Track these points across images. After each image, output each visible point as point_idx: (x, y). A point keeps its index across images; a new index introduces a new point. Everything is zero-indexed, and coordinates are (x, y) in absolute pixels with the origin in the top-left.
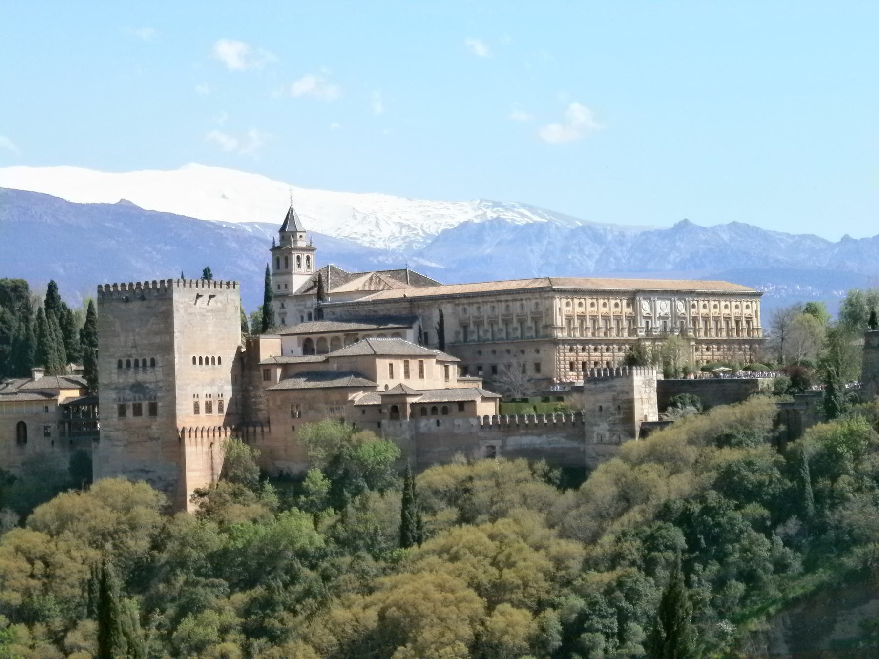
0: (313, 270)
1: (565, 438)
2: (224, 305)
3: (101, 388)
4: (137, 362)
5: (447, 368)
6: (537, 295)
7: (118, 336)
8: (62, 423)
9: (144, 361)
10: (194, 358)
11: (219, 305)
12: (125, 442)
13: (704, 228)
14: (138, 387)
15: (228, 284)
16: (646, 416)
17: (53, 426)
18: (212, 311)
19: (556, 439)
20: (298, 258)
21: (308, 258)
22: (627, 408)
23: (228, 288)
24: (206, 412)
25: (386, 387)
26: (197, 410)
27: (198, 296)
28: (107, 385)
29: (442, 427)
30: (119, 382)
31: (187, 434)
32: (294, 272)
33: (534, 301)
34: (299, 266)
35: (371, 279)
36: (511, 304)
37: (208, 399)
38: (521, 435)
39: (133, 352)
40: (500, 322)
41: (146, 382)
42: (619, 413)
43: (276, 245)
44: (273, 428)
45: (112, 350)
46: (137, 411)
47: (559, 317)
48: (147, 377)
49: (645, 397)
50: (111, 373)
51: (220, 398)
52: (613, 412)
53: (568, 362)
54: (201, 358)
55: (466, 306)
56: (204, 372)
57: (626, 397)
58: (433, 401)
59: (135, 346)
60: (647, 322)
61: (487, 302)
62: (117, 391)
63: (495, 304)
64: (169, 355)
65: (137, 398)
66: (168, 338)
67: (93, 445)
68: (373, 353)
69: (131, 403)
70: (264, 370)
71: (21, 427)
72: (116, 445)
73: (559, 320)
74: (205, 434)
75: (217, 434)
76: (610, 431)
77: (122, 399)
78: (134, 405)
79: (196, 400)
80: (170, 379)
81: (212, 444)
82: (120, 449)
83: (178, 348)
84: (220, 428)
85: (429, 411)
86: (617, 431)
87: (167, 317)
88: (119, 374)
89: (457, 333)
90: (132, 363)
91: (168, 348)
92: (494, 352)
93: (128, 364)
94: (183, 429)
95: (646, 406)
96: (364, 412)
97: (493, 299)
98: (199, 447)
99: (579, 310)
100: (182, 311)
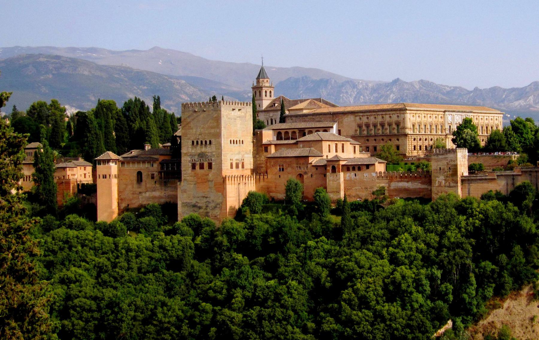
0: (273, 98)
1: (420, 183)
2: (245, 114)
3: (182, 155)
4: (202, 142)
5: (355, 147)
6: (398, 112)
7: (192, 129)
8: (160, 173)
9: (206, 142)
10: (231, 141)
11: (243, 114)
12: (195, 183)
13: (407, 83)
14: (202, 155)
15: (247, 104)
16: (463, 173)
17: (156, 174)
18: (239, 117)
19: (416, 183)
20: (266, 92)
21: (270, 92)
22: (454, 170)
23: (247, 105)
24: (236, 168)
25: (327, 156)
26: (232, 167)
27: (233, 110)
28: (186, 153)
29: (357, 177)
30: (192, 152)
31: (227, 179)
32: (263, 98)
33: (397, 115)
34: (266, 96)
35: (310, 103)
36: (384, 116)
37: (237, 161)
38: (398, 181)
39: (200, 137)
40: (379, 125)
41: (206, 152)
42: (450, 171)
43: (255, 84)
44: (269, 176)
45: (188, 136)
46: (202, 167)
47: (409, 123)
48: (208, 150)
49: (462, 163)
50: (188, 147)
51: (243, 161)
52: (446, 170)
53: (413, 146)
54: (234, 141)
55: (361, 117)
56: (235, 147)
57: (453, 163)
58: (353, 164)
59: (200, 134)
60: (450, 126)
61: (372, 115)
62: (191, 157)
63: (376, 116)
64: (219, 138)
65: (202, 160)
66: (218, 131)
67: (178, 183)
68: (321, 139)
69: (198, 163)
70: (265, 147)
71: (139, 174)
72: (190, 184)
73: (409, 125)
74: (236, 179)
75: (241, 179)
76: (445, 180)
77: (194, 160)
78: (200, 164)
79: (231, 161)
80: (219, 151)
81: (239, 184)
82: (192, 186)
83: (224, 135)
84: (242, 176)
85: (351, 169)
86: (448, 180)
87: (218, 120)
88: (192, 148)
89: (356, 131)
90: (200, 143)
91: (218, 135)
92: (375, 140)
93: (197, 142)
94: (226, 176)
95: (463, 168)
96: (317, 169)
97: (375, 114)
98: (233, 185)
99: (418, 120)
100: (225, 117)
